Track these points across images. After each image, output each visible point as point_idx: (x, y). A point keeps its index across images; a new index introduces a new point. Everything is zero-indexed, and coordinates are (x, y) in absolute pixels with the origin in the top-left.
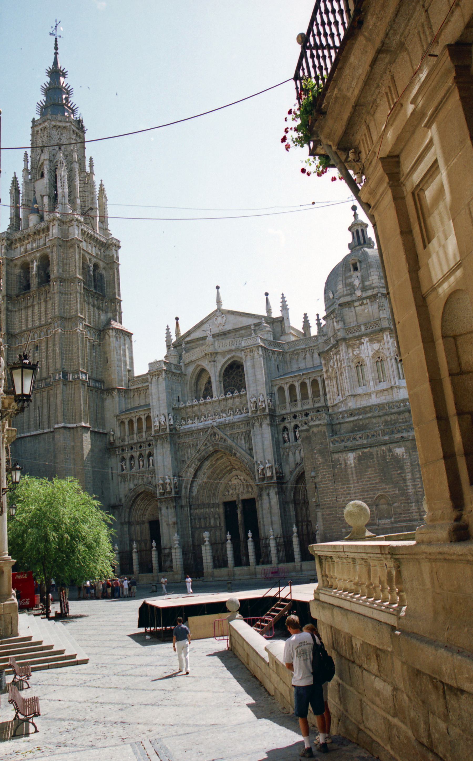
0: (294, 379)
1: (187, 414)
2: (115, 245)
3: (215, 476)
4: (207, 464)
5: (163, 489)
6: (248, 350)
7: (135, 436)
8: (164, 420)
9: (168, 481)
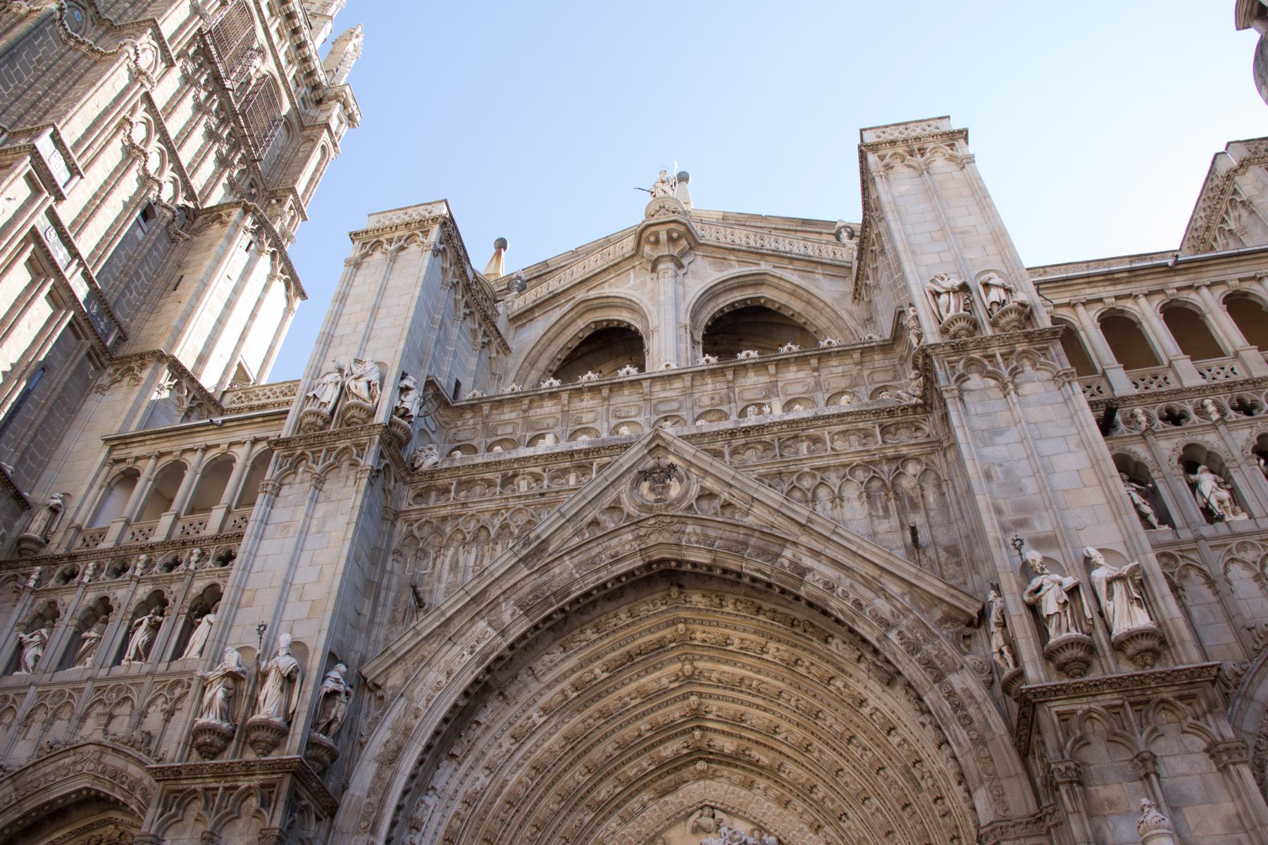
0: (1121, 289)
1: (490, 431)
2: (345, 106)
3: (577, 775)
4: (558, 669)
5: (226, 714)
6: (901, 149)
7: (166, 520)
8: (374, 378)
9: (285, 662)
